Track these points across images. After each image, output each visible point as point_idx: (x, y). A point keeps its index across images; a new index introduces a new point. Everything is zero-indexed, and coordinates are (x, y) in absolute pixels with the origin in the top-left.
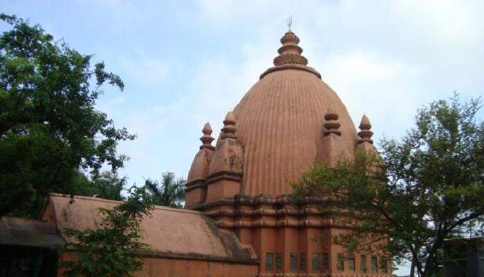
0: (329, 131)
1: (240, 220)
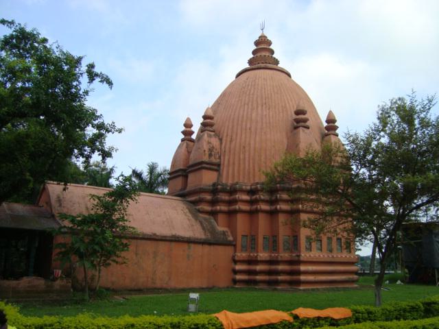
0: (329, 132)
1: (278, 204)
